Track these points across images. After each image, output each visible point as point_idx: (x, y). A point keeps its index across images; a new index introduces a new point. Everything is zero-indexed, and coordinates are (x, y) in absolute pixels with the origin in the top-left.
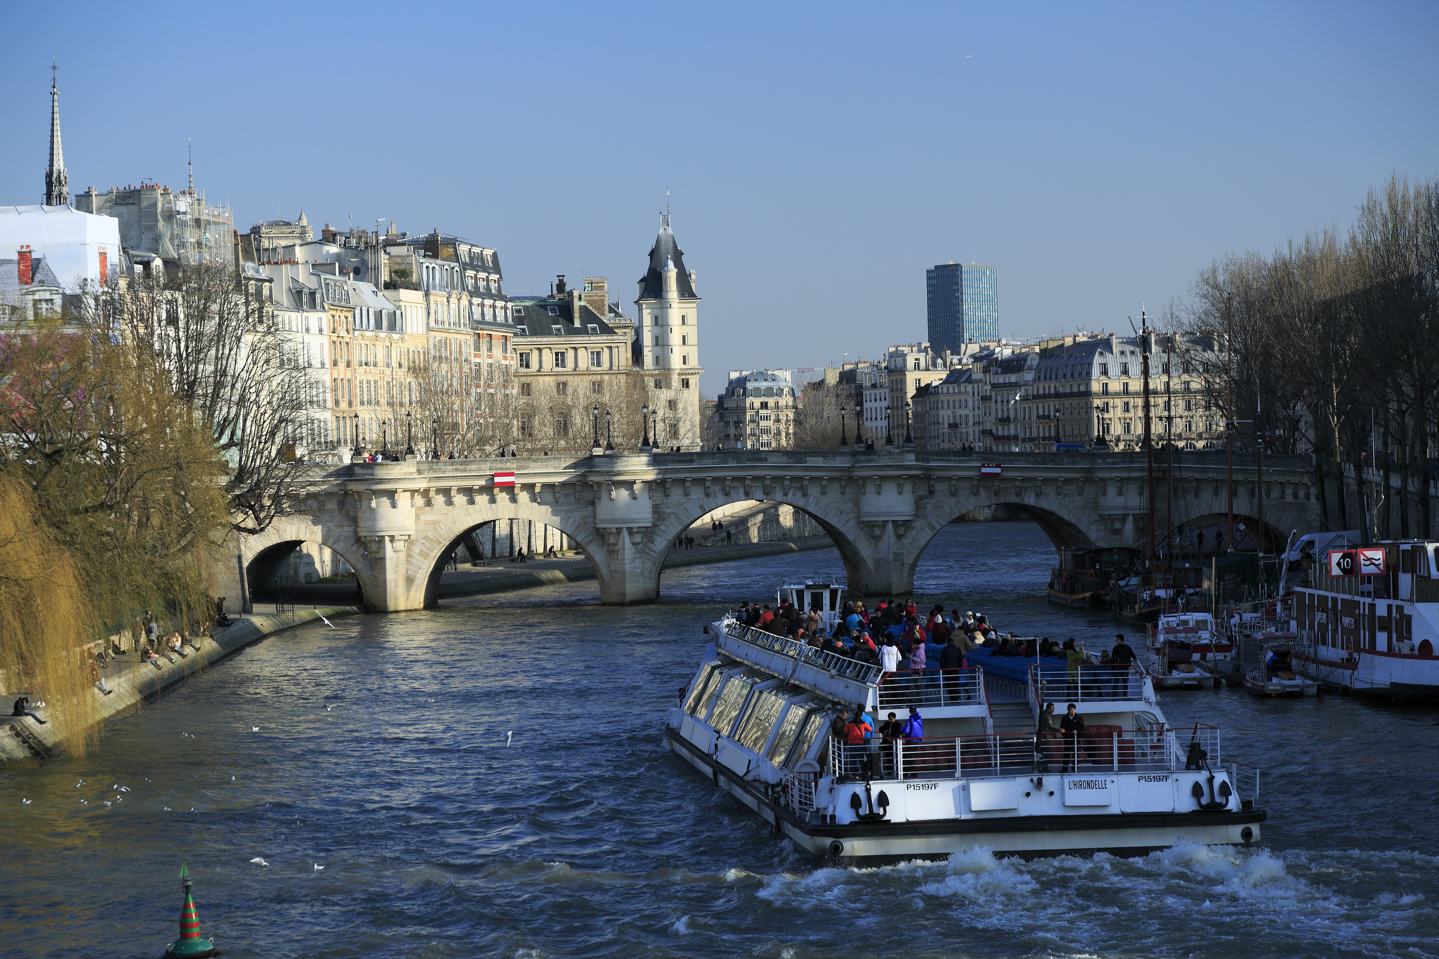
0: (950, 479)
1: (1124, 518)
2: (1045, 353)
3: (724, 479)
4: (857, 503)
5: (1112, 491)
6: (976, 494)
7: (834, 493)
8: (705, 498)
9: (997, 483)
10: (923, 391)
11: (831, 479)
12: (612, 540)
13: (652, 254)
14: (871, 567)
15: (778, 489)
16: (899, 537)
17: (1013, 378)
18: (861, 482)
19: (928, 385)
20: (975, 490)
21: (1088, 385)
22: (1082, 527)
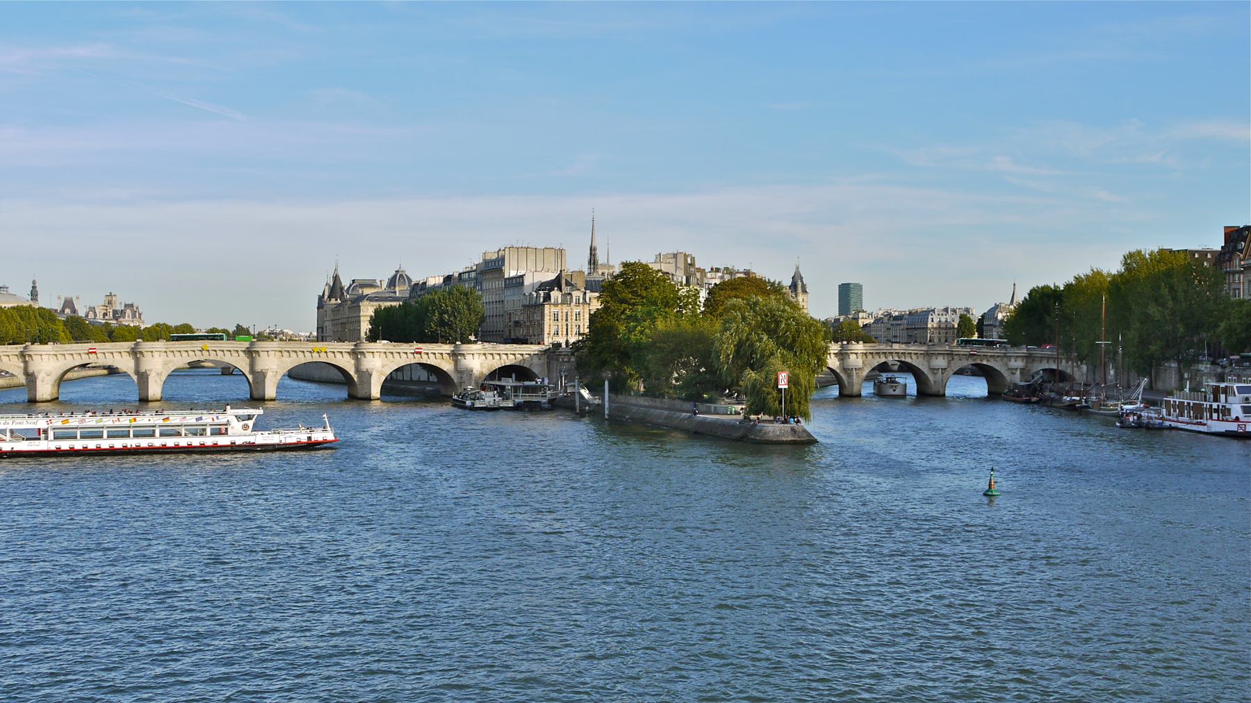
0: (959, 355)
1: (1017, 369)
2: (910, 313)
3: (886, 353)
4: (929, 362)
5: (1013, 360)
6: (967, 360)
7: (921, 358)
10: (865, 326)
12: (849, 372)
13: (793, 278)
16: (942, 373)
17: (899, 322)
19: (867, 324)
21: (927, 325)
22: (1002, 372)
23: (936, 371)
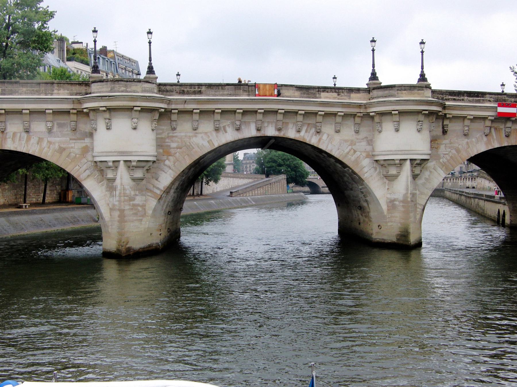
4: (370, 142)
8: (214, 133)
9: (509, 124)
11: (346, 116)
12: (110, 175)
14: (384, 207)
15: (291, 126)
16: (415, 177)
18: (377, 119)
20: (487, 131)
23: (393, 171)
